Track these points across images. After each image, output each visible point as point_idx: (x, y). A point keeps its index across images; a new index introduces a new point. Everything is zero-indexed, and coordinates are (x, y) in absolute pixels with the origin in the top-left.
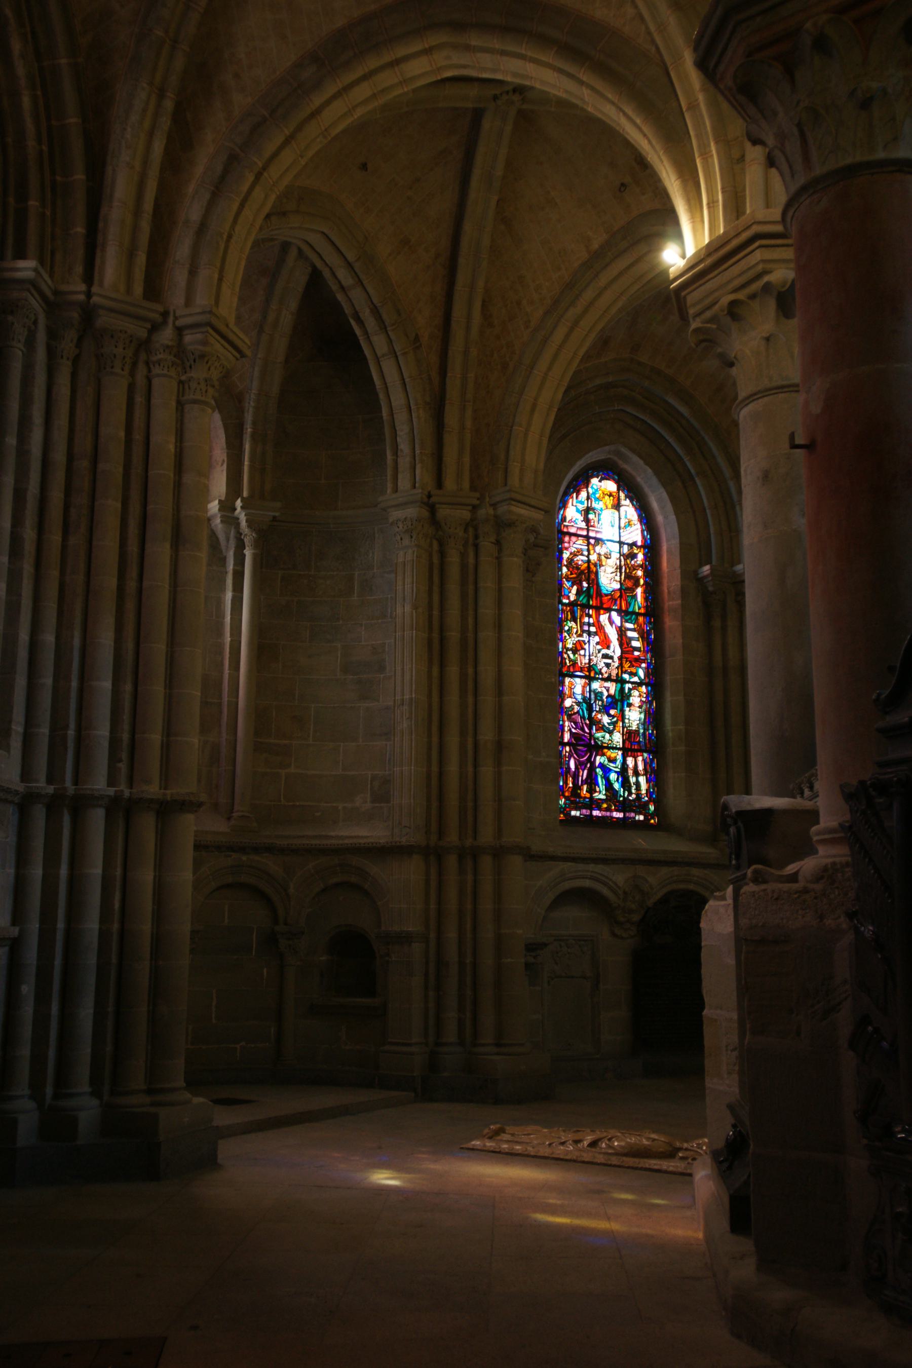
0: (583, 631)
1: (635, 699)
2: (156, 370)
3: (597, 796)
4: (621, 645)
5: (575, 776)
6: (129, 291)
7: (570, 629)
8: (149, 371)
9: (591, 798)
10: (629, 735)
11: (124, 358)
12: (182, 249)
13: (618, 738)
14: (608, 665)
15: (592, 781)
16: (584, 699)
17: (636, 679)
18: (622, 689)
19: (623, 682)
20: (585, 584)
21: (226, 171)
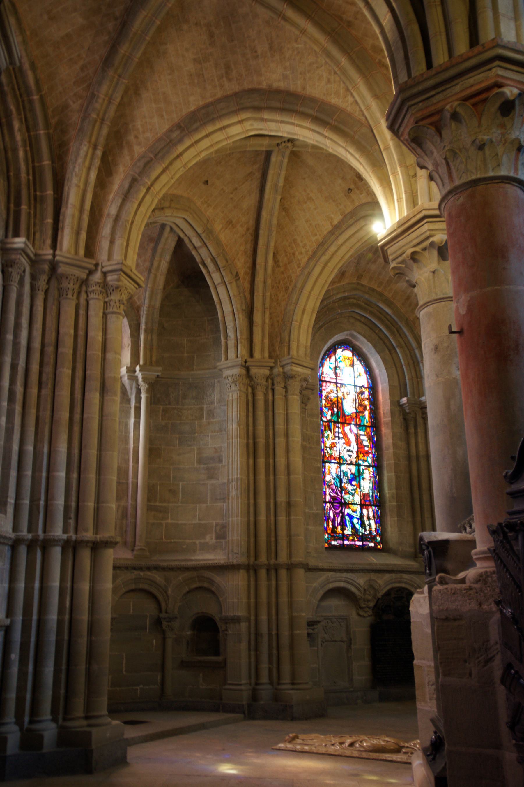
0: (335, 437)
2: (91, 296)
3: (346, 532)
4: (357, 444)
5: (333, 521)
6: (76, 252)
7: (328, 436)
8: (88, 296)
9: (343, 534)
10: (364, 497)
11: (73, 290)
12: (106, 230)
13: (357, 499)
14: (350, 456)
15: (343, 524)
16: (337, 476)
17: (366, 464)
18: (359, 470)
19: (359, 465)
20: (336, 410)
21: (130, 187)
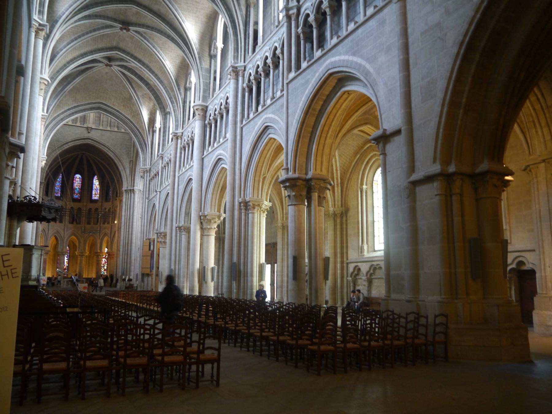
1: (106, 266)
